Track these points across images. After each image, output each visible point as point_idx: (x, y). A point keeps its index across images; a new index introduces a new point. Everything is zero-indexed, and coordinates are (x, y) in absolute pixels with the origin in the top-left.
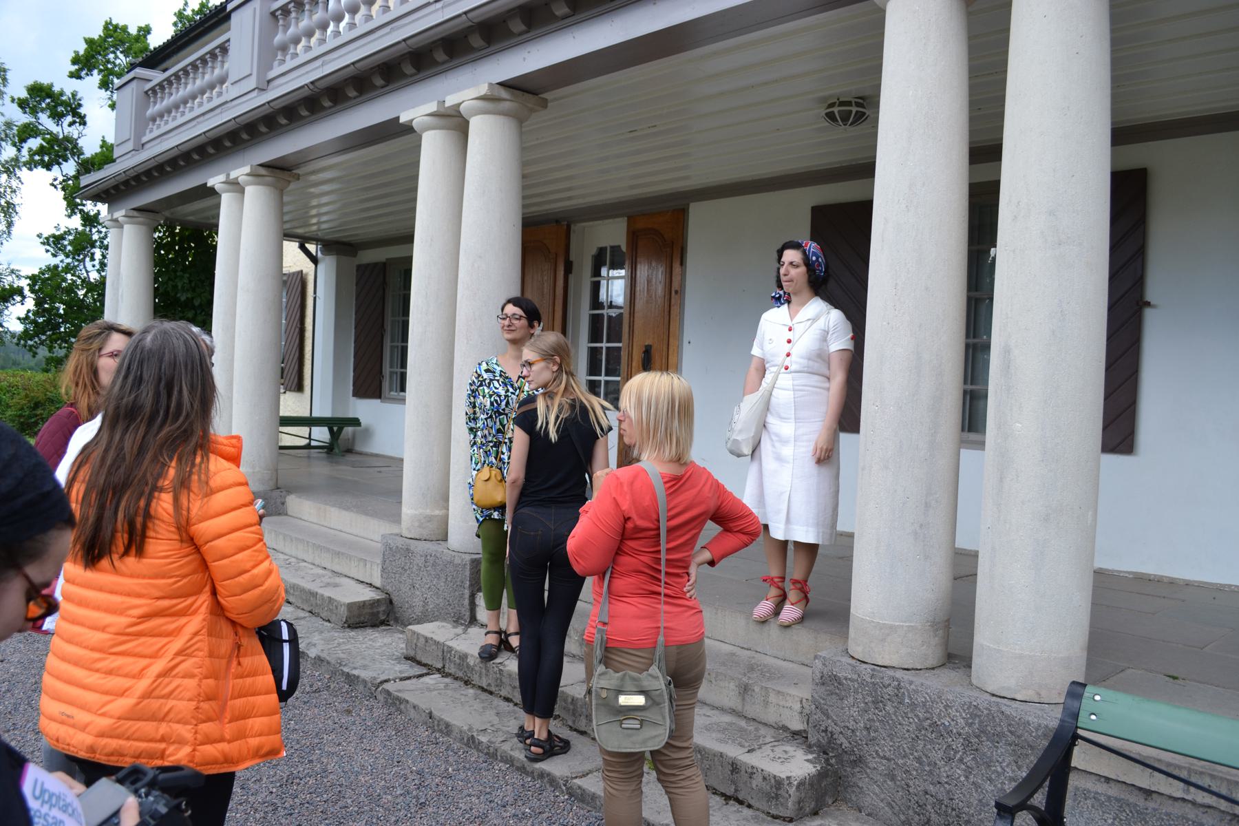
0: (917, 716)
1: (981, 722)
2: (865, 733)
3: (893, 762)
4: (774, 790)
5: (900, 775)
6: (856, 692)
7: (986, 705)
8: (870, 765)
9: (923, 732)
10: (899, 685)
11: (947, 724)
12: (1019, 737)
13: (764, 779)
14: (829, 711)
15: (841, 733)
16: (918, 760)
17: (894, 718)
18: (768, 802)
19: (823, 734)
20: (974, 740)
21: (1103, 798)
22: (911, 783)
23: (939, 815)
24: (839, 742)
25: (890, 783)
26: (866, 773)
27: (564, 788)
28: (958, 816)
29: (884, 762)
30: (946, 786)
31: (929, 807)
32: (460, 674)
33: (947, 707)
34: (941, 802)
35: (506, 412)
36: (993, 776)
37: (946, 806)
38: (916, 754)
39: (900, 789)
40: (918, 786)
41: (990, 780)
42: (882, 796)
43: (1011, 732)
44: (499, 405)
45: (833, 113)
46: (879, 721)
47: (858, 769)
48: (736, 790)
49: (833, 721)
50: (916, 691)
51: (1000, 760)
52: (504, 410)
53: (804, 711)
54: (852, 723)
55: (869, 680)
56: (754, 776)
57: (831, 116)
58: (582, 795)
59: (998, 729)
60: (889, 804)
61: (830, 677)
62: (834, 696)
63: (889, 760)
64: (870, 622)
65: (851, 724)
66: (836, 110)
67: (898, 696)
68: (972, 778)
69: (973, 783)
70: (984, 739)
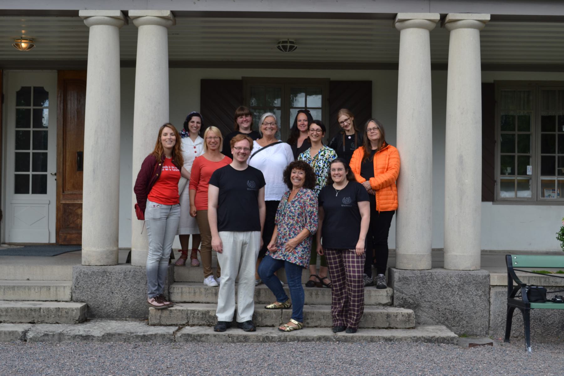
0: (440, 283)
1: (463, 280)
2: (419, 295)
3: (431, 302)
4: (407, 318)
5: (434, 306)
6: (414, 281)
7: (464, 273)
8: (423, 306)
9: (443, 288)
10: (431, 274)
11: (451, 283)
12: (477, 281)
13: (403, 316)
14: (403, 291)
15: (409, 298)
16: (442, 299)
17: (431, 286)
18: (405, 324)
19: (402, 300)
20: (461, 286)
21: (504, 293)
22: (440, 307)
23: (451, 315)
24: (408, 301)
25: (431, 310)
26: (421, 309)
27: (334, 339)
28: (458, 313)
29: (428, 303)
30: (453, 304)
31: (447, 314)
32: (204, 322)
33: (451, 277)
34: (451, 310)
35: (322, 175)
36: (469, 296)
37: (454, 311)
38: (441, 297)
39: (435, 311)
40: (442, 307)
41: (468, 297)
42: (428, 316)
43: (474, 280)
44: (319, 172)
45: (279, 46)
46: (425, 289)
47: (417, 309)
48: (389, 324)
49: (406, 294)
50: (438, 275)
51: (471, 290)
52: (320, 174)
53: (389, 295)
54: (414, 292)
55: (420, 275)
56: (398, 316)
57: (279, 47)
58: (345, 339)
59: (470, 280)
60: (431, 318)
61: (403, 278)
62: (405, 285)
63: (430, 302)
64: (415, 255)
65: (414, 293)
66: (280, 45)
67: (432, 279)
68: (462, 299)
69: (463, 300)
70: (465, 284)
